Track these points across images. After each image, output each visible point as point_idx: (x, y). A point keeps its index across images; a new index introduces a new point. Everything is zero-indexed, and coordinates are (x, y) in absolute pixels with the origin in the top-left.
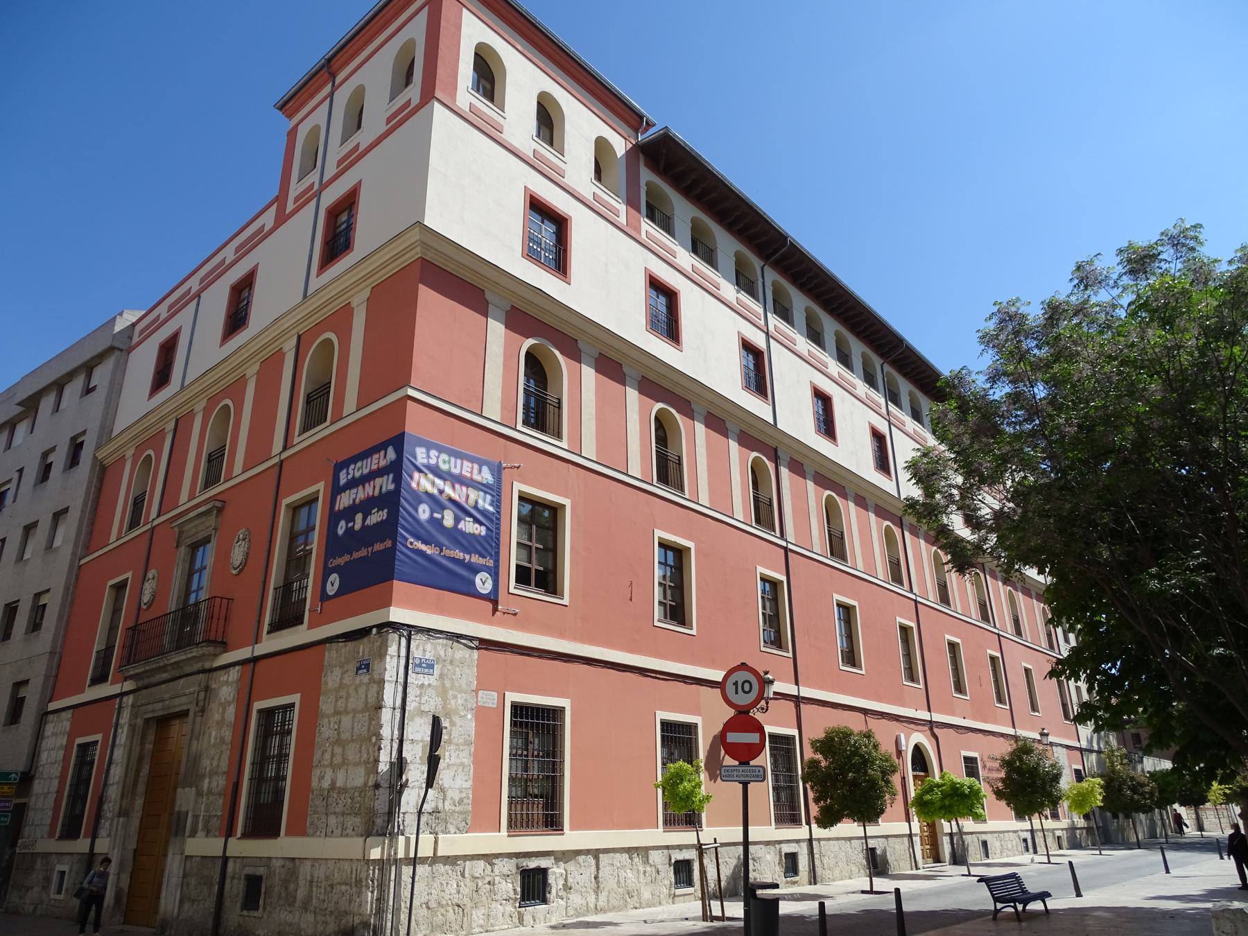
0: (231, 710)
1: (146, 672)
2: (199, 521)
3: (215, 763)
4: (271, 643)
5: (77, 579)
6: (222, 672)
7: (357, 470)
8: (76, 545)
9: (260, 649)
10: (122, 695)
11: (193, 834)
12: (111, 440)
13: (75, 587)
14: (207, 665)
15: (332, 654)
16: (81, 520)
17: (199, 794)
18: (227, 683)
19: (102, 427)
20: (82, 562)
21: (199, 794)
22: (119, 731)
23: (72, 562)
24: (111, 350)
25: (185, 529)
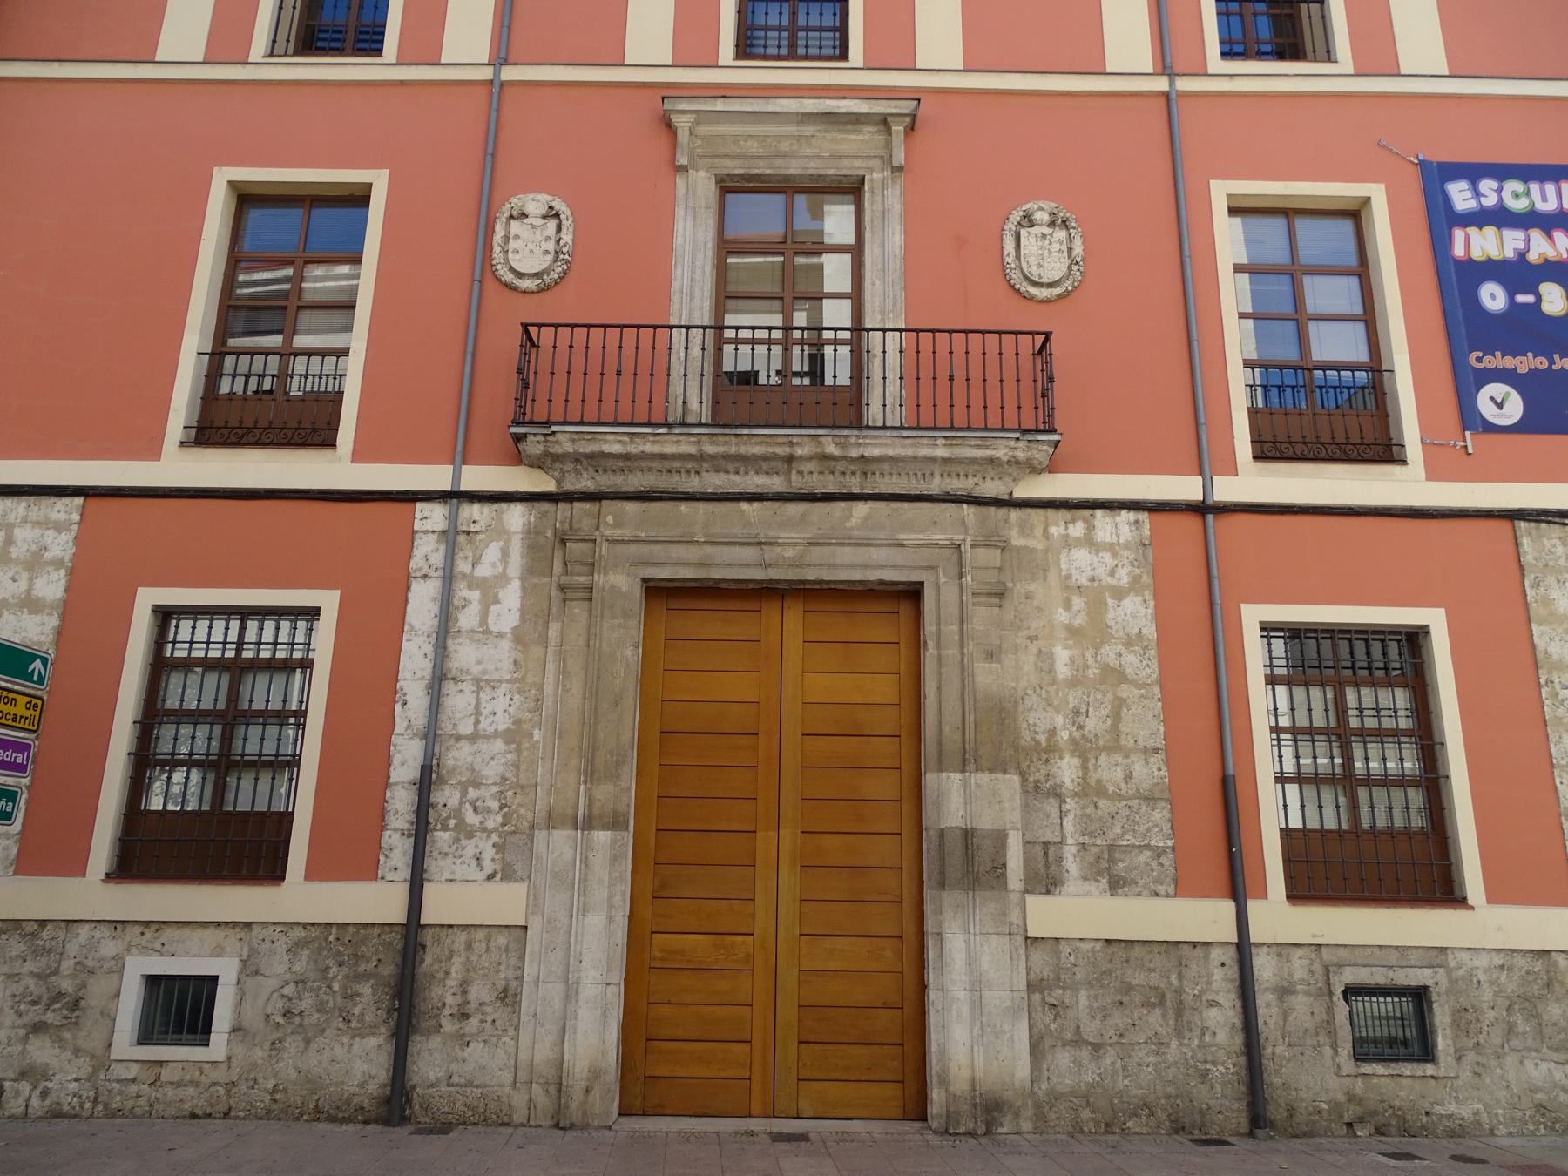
0: (1135, 614)
1: (701, 457)
2: (791, 129)
3: (1095, 724)
6: (1064, 514)
7: (1515, 196)
9: (1226, 490)
11: (1045, 880)
14: (991, 488)
15: (1536, 544)
17: (1038, 791)
18: (1089, 541)
21: (1038, 791)
22: (462, 591)
25: (704, 130)
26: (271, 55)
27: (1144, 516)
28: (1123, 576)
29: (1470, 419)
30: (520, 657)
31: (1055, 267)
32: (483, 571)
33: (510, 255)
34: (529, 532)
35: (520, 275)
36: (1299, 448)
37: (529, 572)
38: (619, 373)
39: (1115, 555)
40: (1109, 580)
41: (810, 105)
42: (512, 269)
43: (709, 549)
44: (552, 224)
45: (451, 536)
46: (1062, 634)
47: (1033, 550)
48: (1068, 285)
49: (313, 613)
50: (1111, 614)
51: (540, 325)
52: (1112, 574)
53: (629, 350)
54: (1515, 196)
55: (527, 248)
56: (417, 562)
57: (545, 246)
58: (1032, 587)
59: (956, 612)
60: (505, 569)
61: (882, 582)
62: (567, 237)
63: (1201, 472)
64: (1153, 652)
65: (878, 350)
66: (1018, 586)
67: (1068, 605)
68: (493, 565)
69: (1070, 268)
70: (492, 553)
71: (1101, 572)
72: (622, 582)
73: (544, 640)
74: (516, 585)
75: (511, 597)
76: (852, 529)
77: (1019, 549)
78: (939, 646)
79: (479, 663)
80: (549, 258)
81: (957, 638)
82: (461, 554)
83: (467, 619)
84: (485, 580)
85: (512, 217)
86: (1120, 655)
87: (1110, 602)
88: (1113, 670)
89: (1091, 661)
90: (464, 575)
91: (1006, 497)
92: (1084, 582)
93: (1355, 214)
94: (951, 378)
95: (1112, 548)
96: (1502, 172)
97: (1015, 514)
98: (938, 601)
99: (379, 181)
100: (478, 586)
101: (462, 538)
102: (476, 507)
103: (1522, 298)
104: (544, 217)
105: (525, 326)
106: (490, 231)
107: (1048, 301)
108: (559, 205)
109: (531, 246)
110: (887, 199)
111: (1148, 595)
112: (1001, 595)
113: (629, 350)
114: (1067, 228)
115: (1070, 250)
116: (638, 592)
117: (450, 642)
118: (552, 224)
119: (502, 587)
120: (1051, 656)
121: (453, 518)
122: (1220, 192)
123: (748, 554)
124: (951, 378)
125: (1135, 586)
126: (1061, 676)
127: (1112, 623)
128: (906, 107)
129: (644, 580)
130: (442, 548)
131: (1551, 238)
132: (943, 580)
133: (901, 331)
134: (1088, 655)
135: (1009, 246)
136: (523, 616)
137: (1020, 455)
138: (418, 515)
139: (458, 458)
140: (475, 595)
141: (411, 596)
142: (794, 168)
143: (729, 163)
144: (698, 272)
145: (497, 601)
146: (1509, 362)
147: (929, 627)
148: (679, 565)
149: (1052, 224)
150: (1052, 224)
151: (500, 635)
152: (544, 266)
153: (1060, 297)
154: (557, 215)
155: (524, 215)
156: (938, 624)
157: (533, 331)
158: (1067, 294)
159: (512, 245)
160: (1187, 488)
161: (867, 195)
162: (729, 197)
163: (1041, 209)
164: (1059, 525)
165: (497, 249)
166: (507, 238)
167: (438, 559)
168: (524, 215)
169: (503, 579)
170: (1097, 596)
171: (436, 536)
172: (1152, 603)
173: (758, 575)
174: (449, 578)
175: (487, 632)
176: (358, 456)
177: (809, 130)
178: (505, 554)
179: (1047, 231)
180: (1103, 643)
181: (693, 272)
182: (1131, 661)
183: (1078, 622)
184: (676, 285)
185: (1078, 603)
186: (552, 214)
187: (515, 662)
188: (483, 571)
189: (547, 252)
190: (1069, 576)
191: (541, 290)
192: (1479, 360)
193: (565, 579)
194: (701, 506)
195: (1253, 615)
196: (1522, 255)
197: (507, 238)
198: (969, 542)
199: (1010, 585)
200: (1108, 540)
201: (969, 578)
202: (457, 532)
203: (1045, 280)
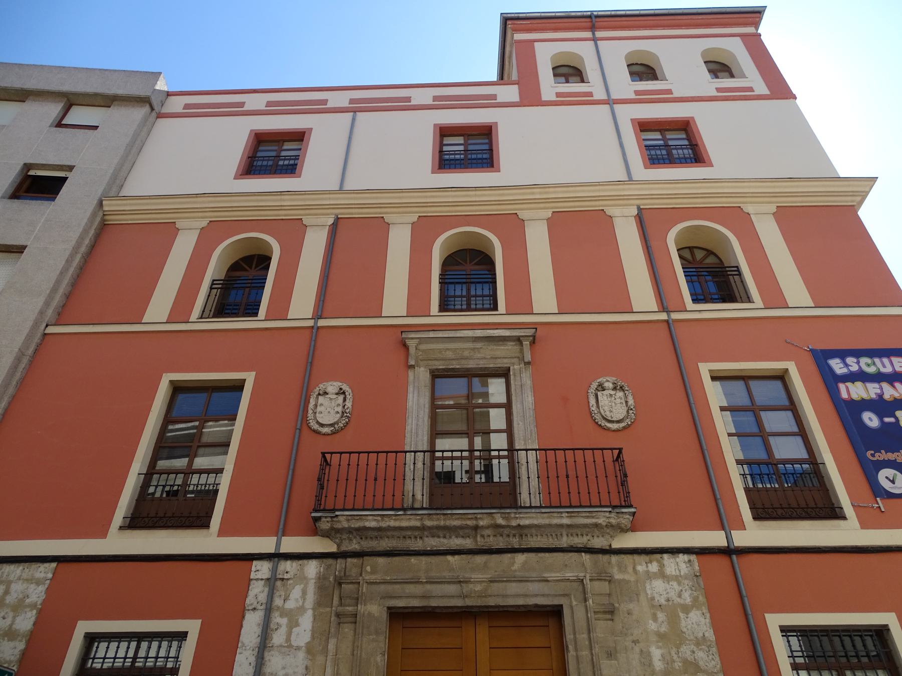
0: (698, 622)
1: (423, 528)
2: (470, 345)
4: (755, 534)
5: (36, 351)
6: (643, 558)
7: (867, 365)
8: (47, 304)
9: (741, 539)
10: (276, 557)
12: (117, 197)
13: (31, 362)
14: (598, 542)
16: (62, 273)
18: (662, 575)
19: (114, 177)
20: (51, 330)
22: (276, 619)
23: (36, 324)
24: (144, 101)
25: (423, 347)
26: (201, 318)
27: (693, 557)
28: (687, 598)
29: (878, 491)
30: (309, 663)
31: (619, 412)
32: (291, 605)
33: (317, 415)
34: (319, 578)
35: (322, 425)
36: (780, 512)
37: (318, 604)
38: (376, 479)
39: (679, 584)
40: (678, 599)
41: (479, 333)
42: (318, 422)
43: (428, 587)
44: (341, 398)
45: (272, 582)
46: (654, 638)
47: (628, 582)
48: (628, 421)
49: (182, 636)
50: (683, 624)
51: (332, 453)
52: (680, 596)
53: (382, 466)
54: (867, 365)
55: (327, 410)
56: (250, 600)
57: (337, 409)
58: (631, 606)
59: (585, 625)
60: (303, 603)
61: (536, 606)
62: (349, 404)
63: (723, 528)
64: (714, 650)
65: (524, 461)
66: (622, 605)
67: (655, 618)
68: (297, 600)
69: (628, 412)
70: (296, 593)
71: (673, 595)
72: (375, 610)
73: (325, 651)
74: (310, 613)
75: (306, 622)
76: (515, 571)
77: (620, 581)
78: (576, 650)
79: (284, 668)
80: (339, 415)
81: (587, 643)
82: (277, 594)
83: (278, 638)
84: (291, 610)
85: (319, 394)
86: (694, 652)
87: (681, 615)
88: (691, 663)
89: (675, 657)
90: (278, 607)
91: (608, 548)
92: (663, 601)
93: (782, 377)
94: (567, 476)
95: (677, 578)
96: (858, 354)
97: (614, 559)
98: (573, 617)
99: (250, 378)
100: (286, 615)
101: (279, 583)
102: (289, 562)
103: (887, 420)
104: (337, 394)
105: (323, 454)
106: (307, 402)
107: (617, 431)
108: (345, 387)
109: (329, 409)
110: (523, 379)
111: (705, 610)
112: (612, 612)
113: (382, 466)
114: (623, 391)
115: (626, 402)
116: (385, 616)
117: (266, 654)
118: (341, 398)
119: (302, 615)
120: (649, 654)
121: (274, 570)
122: (705, 369)
123: (452, 589)
124: (567, 476)
125: (695, 604)
126: (658, 669)
127: (685, 630)
128: (530, 332)
129: (389, 608)
130: (267, 590)
131: (894, 387)
132: (574, 603)
133: (536, 450)
134: (673, 653)
135: (592, 401)
136: (313, 637)
137: (613, 521)
138: (253, 569)
139: (280, 533)
140: (284, 621)
141: (244, 623)
142: (471, 364)
143: (436, 363)
144: (421, 420)
145: (297, 625)
146: (891, 456)
147: (569, 636)
148: (410, 597)
149: (615, 389)
150: (615, 389)
151: (298, 648)
152: (336, 420)
153: (624, 428)
154: (344, 393)
155: (326, 393)
156: (575, 634)
157: (328, 456)
158: (628, 426)
159: (319, 409)
160: (716, 539)
161: (512, 377)
162: (438, 380)
163: (608, 381)
164: (642, 565)
165: (310, 412)
166: (316, 406)
167: (263, 597)
168: (326, 393)
169: (301, 610)
170: (673, 611)
171: (263, 582)
172: (708, 615)
173: (459, 603)
174: (269, 610)
175: (290, 646)
176: (222, 533)
177: (479, 345)
178: (304, 593)
179: (613, 392)
180: (681, 644)
181: (418, 421)
182: (700, 655)
183: (663, 629)
184: (408, 428)
185: (661, 616)
186: (341, 392)
187: (307, 668)
188: (291, 605)
189: (338, 412)
190: (653, 599)
191: (333, 433)
192: (873, 455)
193: (340, 609)
194: (424, 559)
195: (774, 621)
196: (881, 396)
197: (316, 406)
198: (588, 578)
199: (617, 605)
200: (674, 573)
201: (591, 601)
202: (276, 579)
203: (614, 419)
